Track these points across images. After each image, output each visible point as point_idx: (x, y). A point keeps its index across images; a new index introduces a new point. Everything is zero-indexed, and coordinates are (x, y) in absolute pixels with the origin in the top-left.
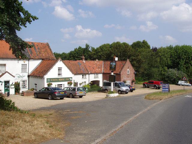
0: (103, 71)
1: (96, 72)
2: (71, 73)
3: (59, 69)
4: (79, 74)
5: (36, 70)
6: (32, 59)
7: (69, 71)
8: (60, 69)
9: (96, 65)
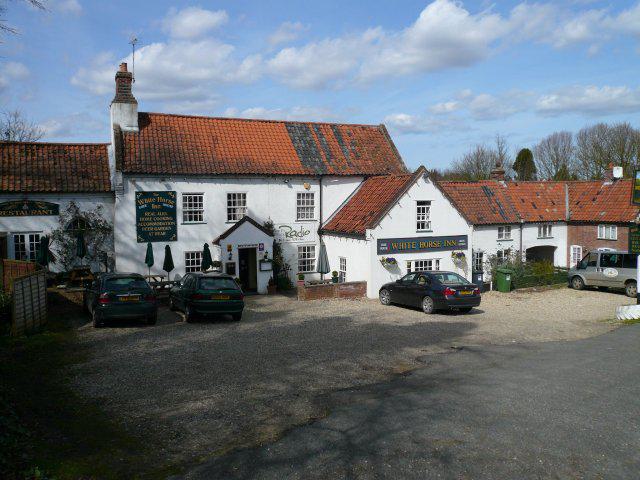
0: (567, 212)
1: (546, 218)
2: (462, 221)
3: (419, 209)
4: (489, 225)
5: (345, 210)
6: (332, 176)
7: (454, 212)
8: (423, 206)
9: (544, 196)
